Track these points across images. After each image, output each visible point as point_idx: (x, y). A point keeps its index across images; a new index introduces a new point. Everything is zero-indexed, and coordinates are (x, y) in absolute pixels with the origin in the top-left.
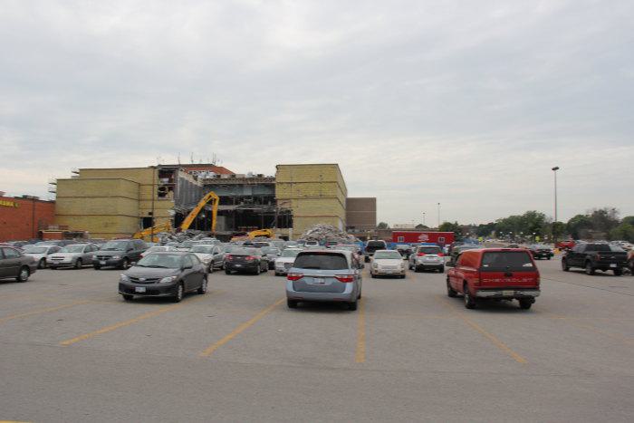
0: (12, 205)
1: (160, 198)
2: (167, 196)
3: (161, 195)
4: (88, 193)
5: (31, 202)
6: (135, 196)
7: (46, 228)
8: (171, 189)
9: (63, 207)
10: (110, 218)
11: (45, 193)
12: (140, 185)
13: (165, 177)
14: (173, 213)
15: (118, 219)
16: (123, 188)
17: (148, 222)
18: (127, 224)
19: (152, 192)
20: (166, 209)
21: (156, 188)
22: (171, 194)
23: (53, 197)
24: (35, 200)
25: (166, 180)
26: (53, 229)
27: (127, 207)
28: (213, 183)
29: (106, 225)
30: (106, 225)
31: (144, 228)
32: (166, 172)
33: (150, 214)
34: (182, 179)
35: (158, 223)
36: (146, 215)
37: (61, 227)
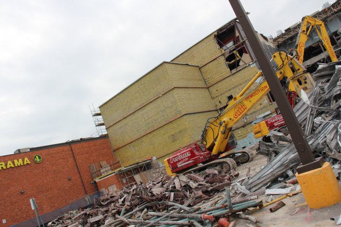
1: (234, 71)
2: (241, 63)
3: (232, 67)
4: (136, 105)
5: (68, 147)
6: (201, 84)
7: (99, 175)
8: (242, 51)
9: (119, 137)
10: (175, 125)
12: (200, 68)
15: (187, 121)
21: (222, 60)
22: (246, 58)
23: (103, 131)
25: (230, 45)
29: (174, 138)
30: (174, 138)
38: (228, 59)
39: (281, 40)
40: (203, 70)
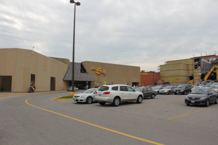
0: (147, 74)
2: (198, 68)
3: (196, 68)
4: (171, 69)
5: (153, 73)
6: (187, 69)
7: (157, 81)
8: (199, 65)
11: (157, 70)
12: (188, 65)
13: (196, 61)
14: (200, 74)
15: (181, 77)
16: (182, 67)
17: (191, 78)
18: (184, 79)
19: (191, 67)
20: (198, 73)
21: (194, 65)
22: (199, 67)
23: (159, 71)
24: (154, 72)
25: (197, 62)
26: (160, 81)
27: (183, 73)
28: (215, 62)
29: (177, 80)
30: (177, 80)
31: (190, 80)
32: (197, 59)
33: (192, 75)
34: (203, 62)
35: (195, 78)
36: (191, 75)
37: (162, 81)
38: (195, 66)
39: (214, 62)
40: (189, 66)
